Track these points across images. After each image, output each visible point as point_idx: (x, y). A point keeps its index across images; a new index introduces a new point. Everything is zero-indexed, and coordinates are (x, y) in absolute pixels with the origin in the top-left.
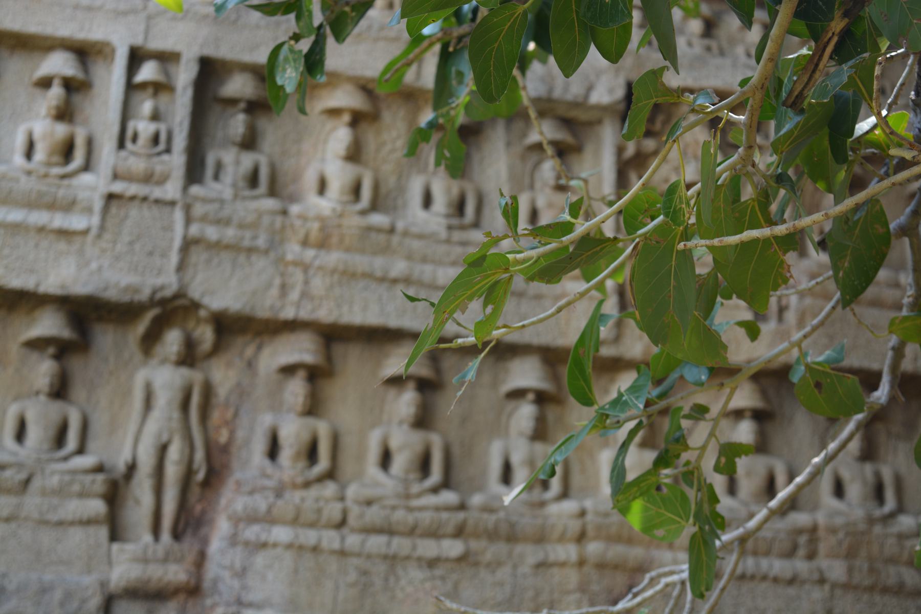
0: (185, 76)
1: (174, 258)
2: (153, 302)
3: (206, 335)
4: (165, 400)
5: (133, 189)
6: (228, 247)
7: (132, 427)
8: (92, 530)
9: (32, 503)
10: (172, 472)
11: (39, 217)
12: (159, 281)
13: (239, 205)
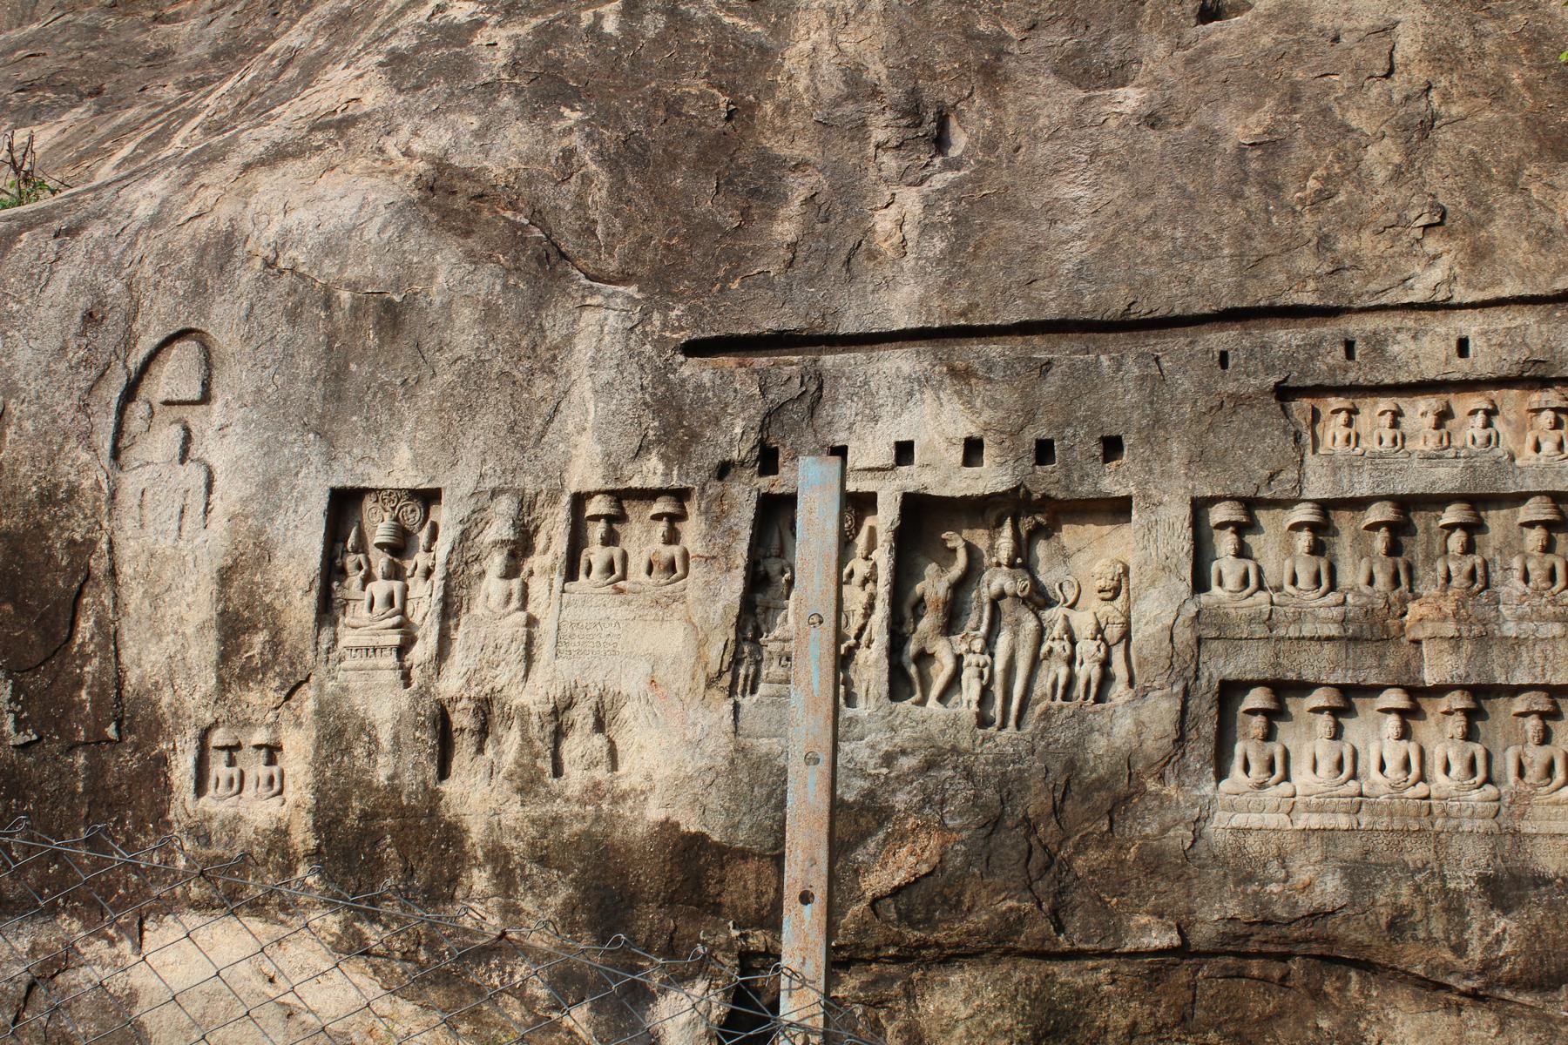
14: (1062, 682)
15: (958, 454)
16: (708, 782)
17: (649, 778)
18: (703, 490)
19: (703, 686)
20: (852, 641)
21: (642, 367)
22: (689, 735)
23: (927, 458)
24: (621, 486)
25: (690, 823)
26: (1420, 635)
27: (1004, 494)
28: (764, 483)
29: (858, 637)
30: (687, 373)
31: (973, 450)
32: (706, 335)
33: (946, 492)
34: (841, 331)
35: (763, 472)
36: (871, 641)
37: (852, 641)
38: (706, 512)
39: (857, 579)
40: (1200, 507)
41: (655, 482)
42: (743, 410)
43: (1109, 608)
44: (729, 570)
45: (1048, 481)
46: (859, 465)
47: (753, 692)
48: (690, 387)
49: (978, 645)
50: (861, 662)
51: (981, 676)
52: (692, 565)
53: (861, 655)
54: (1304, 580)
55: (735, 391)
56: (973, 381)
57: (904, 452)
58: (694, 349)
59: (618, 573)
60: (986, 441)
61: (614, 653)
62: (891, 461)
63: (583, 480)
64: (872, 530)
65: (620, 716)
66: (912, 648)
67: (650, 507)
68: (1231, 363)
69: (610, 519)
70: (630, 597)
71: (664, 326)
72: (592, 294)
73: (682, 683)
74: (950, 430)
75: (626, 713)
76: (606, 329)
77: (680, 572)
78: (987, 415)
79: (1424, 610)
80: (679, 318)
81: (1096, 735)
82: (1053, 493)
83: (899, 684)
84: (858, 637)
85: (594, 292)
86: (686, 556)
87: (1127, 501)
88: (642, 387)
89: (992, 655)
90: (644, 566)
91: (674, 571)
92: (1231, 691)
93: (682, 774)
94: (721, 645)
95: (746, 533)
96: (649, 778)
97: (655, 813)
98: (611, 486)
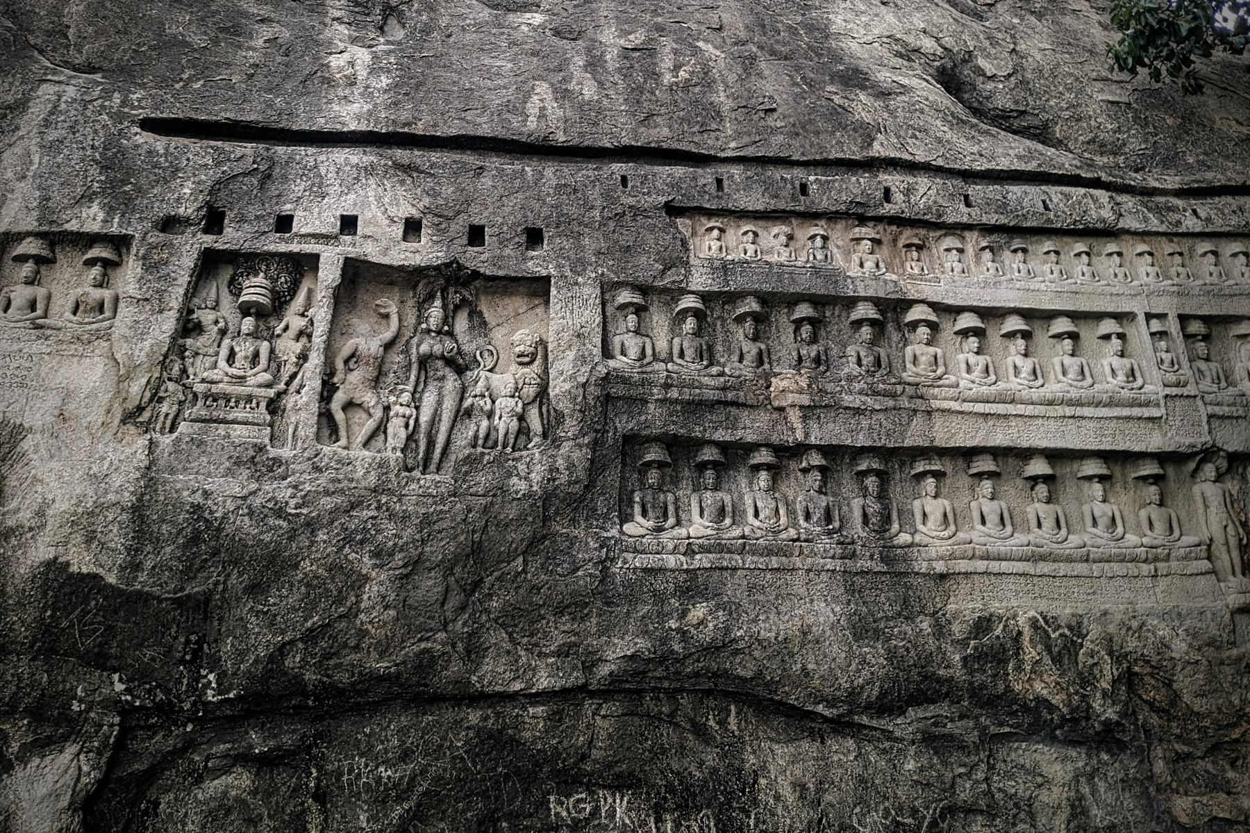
0: (1173, 326)
1: (1206, 427)
2: (1202, 451)
3: (1224, 464)
4: (1215, 502)
5: (1174, 391)
6: (1228, 417)
7: (1202, 519)
8: (1208, 577)
9: (1174, 564)
10: (1233, 542)
11: (1137, 412)
12: (1203, 439)
13: (1223, 393)
14: (482, 434)
15: (399, 230)
16: (110, 518)
17: (40, 513)
18: (144, 238)
19: (116, 422)
20: (282, 386)
21: (96, 132)
22: (95, 469)
23: (368, 232)
24: (55, 229)
25: (81, 561)
26: (784, 404)
27: (437, 268)
28: (208, 240)
29: (288, 384)
30: (141, 141)
31: (412, 228)
32: (165, 115)
33: (385, 261)
34: (295, 128)
35: (206, 231)
36: (302, 386)
37: (282, 386)
38: (144, 258)
39: (292, 333)
40: (607, 288)
41: (94, 227)
42: (195, 175)
43: (526, 370)
44: (161, 312)
45: (479, 259)
46: (303, 231)
47: (172, 430)
48: (143, 151)
49: (406, 397)
50: (289, 406)
51: (407, 426)
52: (122, 305)
53: (290, 401)
54: (689, 353)
55: (188, 159)
56: (415, 175)
57: (349, 224)
58: (149, 125)
59: (39, 312)
60: (424, 222)
61: (22, 385)
62: (337, 230)
63: (16, 221)
64: (310, 291)
65: (18, 449)
66: (339, 398)
67: (83, 254)
68: (630, 185)
69: (39, 260)
70: (49, 332)
71: (124, 103)
72: (54, 74)
73: (96, 417)
74: (393, 211)
75: (27, 444)
76: (64, 99)
77: (107, 314)
78: (426, 201)
79: (785, 383)
80: (139, 100)
81: (515, 480)
82: (482, 270)
83: (328, 425)
84: (288, 384)
85: (55, 73)
86: (116, 300)
87: (547, 279)
88: (93, 147)
89: (417, 408)
90: (70, 305)
91: (101, 311)
92: (632, 442)
93: (80, 510)
94: (144, 381)
95: (184, 279)
96: (40, 513)
97: (41, 551)
98: (45, 228)
